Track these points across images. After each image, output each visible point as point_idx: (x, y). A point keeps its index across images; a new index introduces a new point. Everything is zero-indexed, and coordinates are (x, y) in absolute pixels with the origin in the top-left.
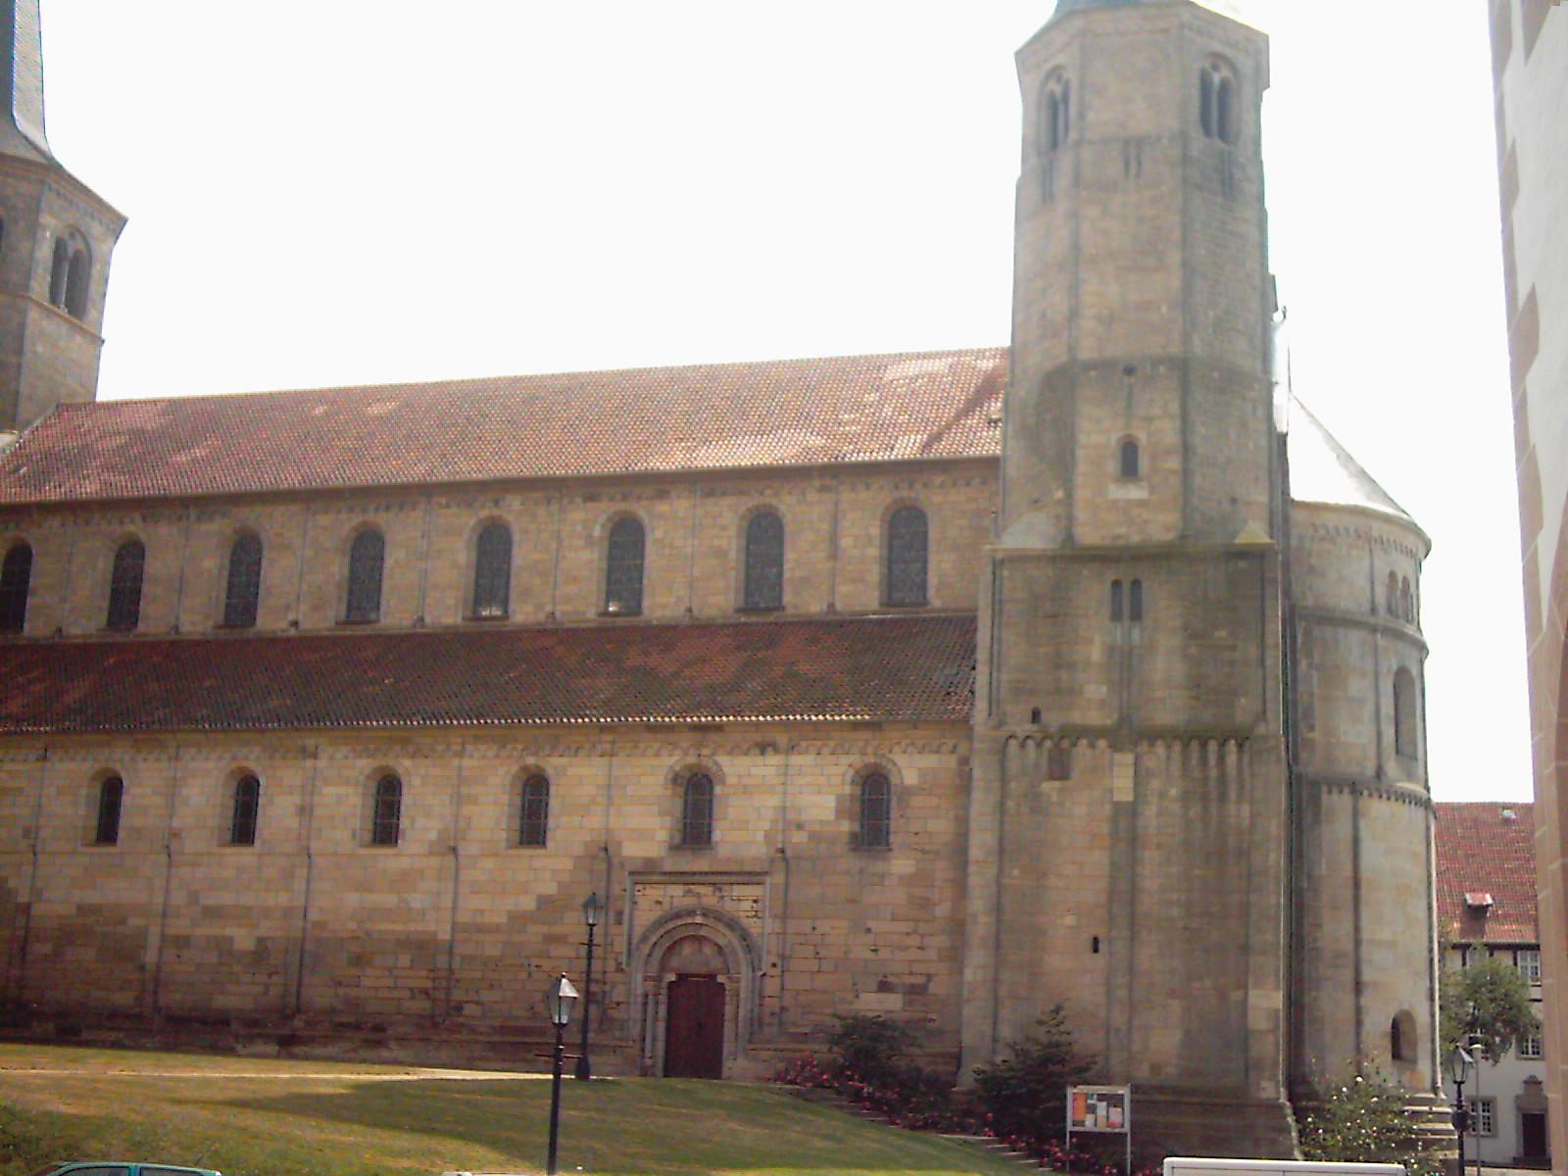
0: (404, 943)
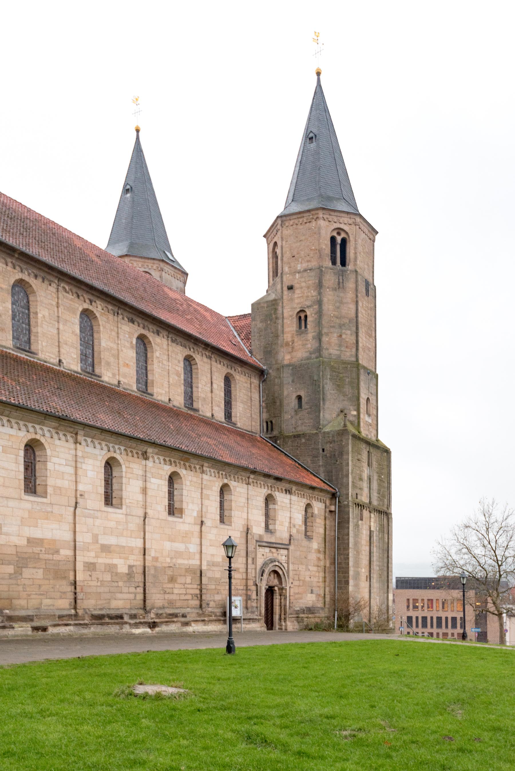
0: (189, 570)
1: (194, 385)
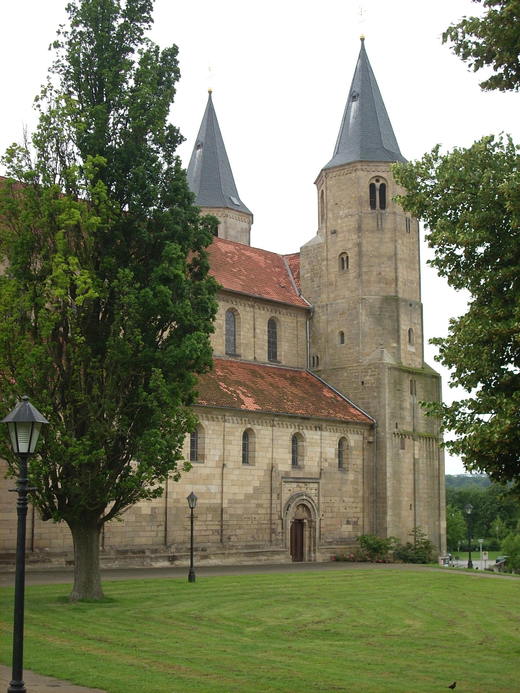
1: (236, 333)
